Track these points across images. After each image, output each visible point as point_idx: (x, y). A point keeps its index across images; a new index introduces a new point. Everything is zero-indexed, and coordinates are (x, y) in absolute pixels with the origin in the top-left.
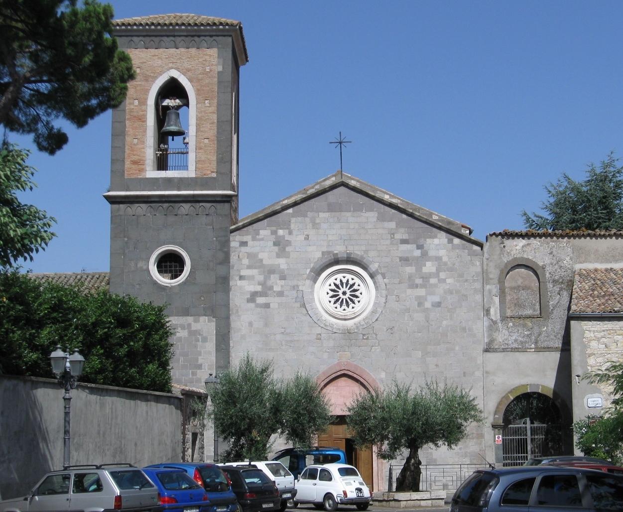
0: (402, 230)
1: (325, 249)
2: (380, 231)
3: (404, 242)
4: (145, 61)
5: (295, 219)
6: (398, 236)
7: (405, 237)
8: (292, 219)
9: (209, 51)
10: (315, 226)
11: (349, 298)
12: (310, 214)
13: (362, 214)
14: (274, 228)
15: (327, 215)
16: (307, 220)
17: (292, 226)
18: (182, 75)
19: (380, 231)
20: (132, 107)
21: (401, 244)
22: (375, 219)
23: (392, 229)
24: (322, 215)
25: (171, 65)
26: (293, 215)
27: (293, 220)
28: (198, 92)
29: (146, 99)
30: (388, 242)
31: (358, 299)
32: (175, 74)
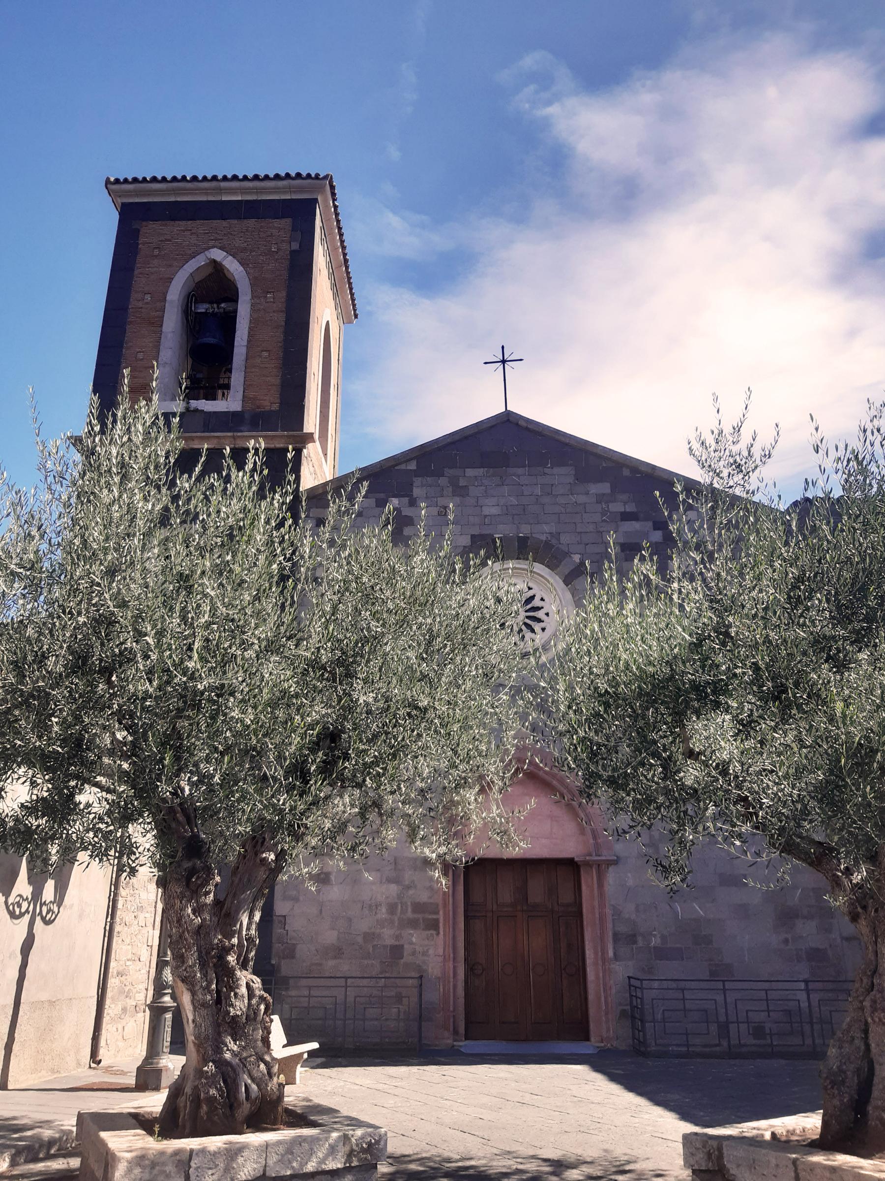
0: (624, 497)
1: (476, 531)
2: (582, 499)
3: (626, 517)
4: (168, 237)
5: (420, 479)
6: (617, 507)
7: (630, 508)
8: (415, 479)
9: (277, 223)
10: (459, 491)
11: (527, 617)
12: (449, 472)
13: (546, 471)
14: (382, 496)
15: (480, 472)
16: (443, 481)
17: (417, 492)
18: (230, 258)
19: (582, 499)
20: (140, 304)
21: (622, 520)
22: (571, 479)
23: (604, 494)
24: (470, 472)
25: (211, 243)
26: (417, 473)
27: (418, 481)
28: (254, 283)
29: (165, 295)
30: (597, 518)
31: (542, 625)
32: (217, 254)
